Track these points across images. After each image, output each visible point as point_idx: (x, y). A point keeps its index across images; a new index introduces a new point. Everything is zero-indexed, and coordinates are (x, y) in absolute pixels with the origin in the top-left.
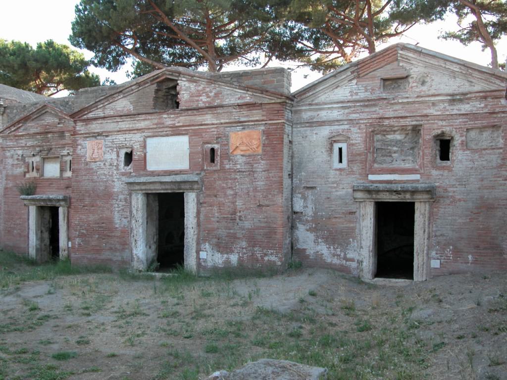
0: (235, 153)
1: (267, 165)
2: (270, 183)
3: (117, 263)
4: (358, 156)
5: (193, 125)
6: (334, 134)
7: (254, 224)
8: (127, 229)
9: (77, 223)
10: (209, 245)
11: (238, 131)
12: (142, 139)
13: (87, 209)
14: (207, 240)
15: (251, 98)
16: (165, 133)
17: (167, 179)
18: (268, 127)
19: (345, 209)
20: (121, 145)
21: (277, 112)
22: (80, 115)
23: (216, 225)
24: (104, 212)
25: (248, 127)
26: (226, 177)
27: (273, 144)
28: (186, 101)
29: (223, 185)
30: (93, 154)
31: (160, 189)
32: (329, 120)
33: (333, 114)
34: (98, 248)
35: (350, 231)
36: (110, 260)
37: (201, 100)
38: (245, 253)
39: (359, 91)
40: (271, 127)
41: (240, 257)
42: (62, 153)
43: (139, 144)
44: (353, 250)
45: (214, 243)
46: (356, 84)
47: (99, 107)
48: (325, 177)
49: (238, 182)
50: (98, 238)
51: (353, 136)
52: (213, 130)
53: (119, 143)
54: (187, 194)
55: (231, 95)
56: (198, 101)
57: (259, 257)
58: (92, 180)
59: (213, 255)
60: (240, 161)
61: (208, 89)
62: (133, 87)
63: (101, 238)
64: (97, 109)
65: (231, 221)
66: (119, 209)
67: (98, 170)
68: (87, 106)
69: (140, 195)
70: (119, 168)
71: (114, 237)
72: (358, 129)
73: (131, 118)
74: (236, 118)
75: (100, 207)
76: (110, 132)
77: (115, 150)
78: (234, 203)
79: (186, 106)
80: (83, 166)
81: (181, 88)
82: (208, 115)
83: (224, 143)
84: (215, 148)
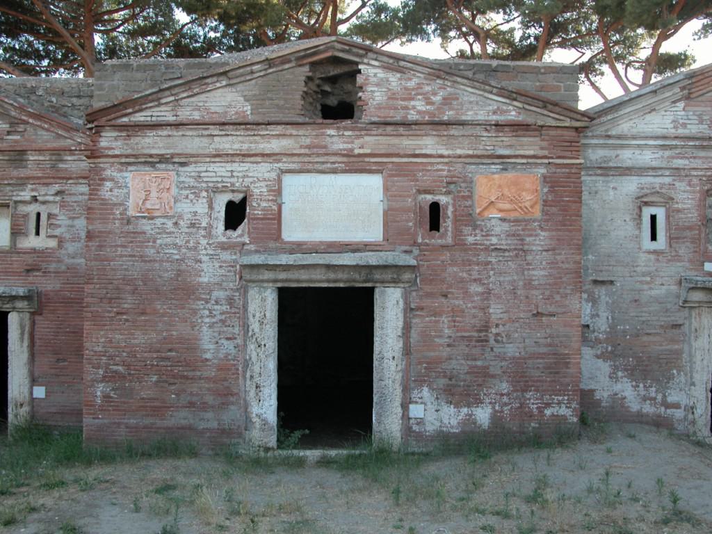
0: (486, 214)
1: (551, 238)
2: (558, 273)
3: (208, 434)
4: (688, 231)
5: (398, 155)
6: (646, 191)
7: (525, 348)
8: (232, 362)
9: (100, 349)
10: (429, 391)
11: (493, 173)
12: (273, 175)
13: (127, 320)
14: (425, 381)
15: (520, 113)
16: (329, 165)
17: (347, 259)
18: (554, 170)
19: (665, 319)
20: (220, 185)
21: (569, 144)
22: (113, 116)
23: (446, 352)
24: (174, 326)
25: (513, 168)
26: (469, 260)
27: (563, 201)
28: (379, 107)
29: (461, 274)
30: (146, 200)
31: (304, 279)
32: (637, 166)
33: (644, 157)
34: (157, 404)
35: (674, 356)
36: (190, 428)
37: (414, 107)
38: (506, 404)
39: (689, 122)
40: (558, 170)
41: (496, 411)
42: (18, 195)
43: (267, 186)
44: (678, 390)
45: (441, 386)
46: (684, 110)
47: (163, 101)
48: (631, 263)
49: (492, 269)
50: (157, 382)
51: (680, 196)
52: (440, 167)
53: (215, 179)
54: (383, 293)
55: (477, 103)
56: (406, 108)
57: (535, 410)
58: (141, 256)
59: (437, 411)
60: (498, 232)
61: (427, 88)
62: (255, 68)
63: (164, 382)
64: (158, 106)
65: (478, 344)
66: (214, 320)
67: (159, 236)
68: (136, 96)
69: (269, 290)
70: (214, 232)
71: (200, 379)
72: (687, 185)
73: (247, 129)
74: (488, 148)
75: (163, 315)
76: (193, 156)
77: (204, 194)
78: (484, 309)
79: (379, 117)
80: (117, 225)
81: (366, 79)
82: (429, 138)
83: (462, 194)
84: (441, 203)
